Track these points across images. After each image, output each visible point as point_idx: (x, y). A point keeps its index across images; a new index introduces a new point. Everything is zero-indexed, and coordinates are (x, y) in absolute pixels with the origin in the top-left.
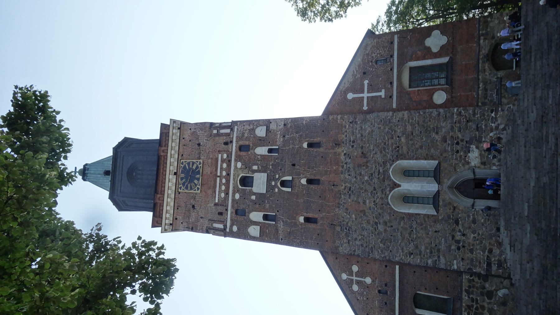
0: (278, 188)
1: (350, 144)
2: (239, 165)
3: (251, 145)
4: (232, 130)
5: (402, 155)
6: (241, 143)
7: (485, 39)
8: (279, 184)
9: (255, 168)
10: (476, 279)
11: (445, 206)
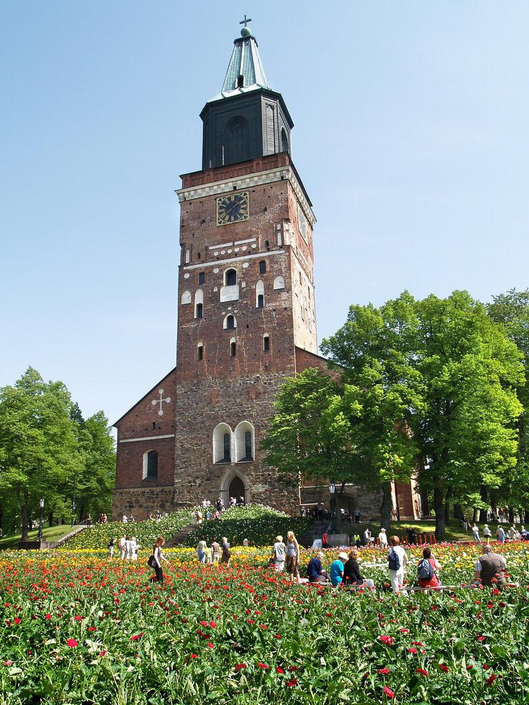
0: (226, 315)
1: (267, 380)
2: (246, 265)
3: (265, 275)
4: (281, 247)
5: (259, 430)
6: (267, 262)
7: (358, 489)
8: (230, 314)
9: (244, 285)
10: (171, 496)
11: (220, 470)
